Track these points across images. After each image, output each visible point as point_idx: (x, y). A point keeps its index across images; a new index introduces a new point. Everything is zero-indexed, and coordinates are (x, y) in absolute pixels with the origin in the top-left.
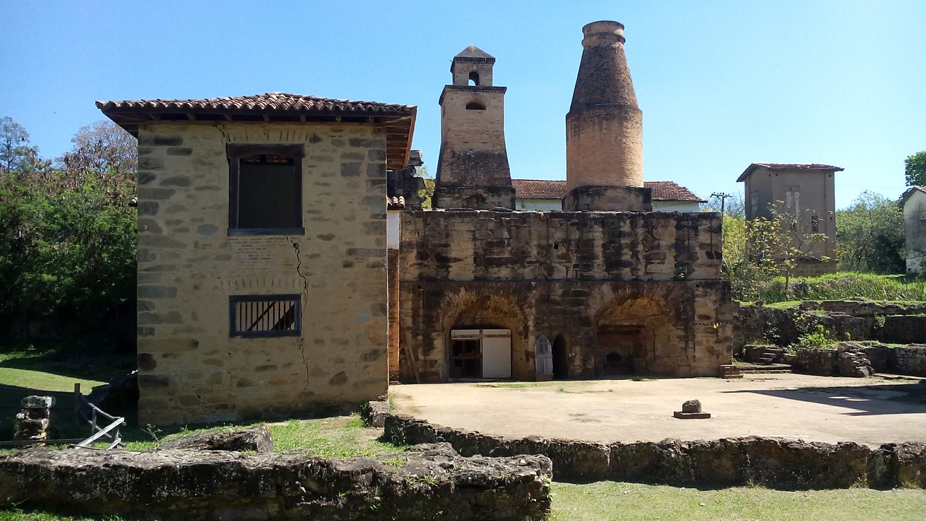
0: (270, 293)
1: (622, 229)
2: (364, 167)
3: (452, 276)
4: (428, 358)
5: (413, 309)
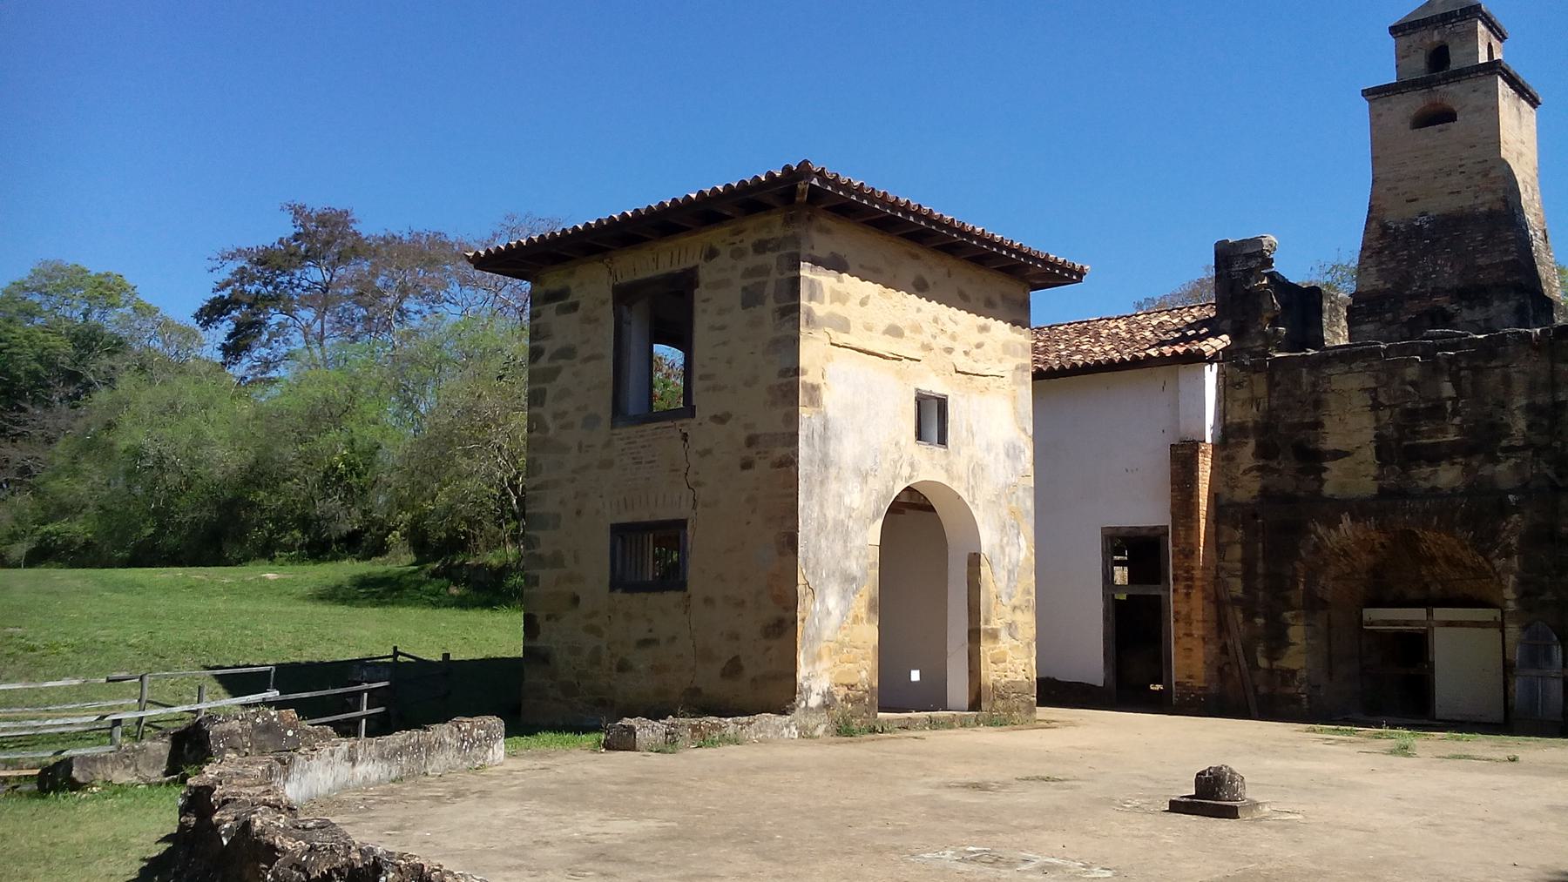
0: (653, 519)
2: (770, 289)
3: (1328, 490)
4: (1275, 664)
5: (1243, 561)
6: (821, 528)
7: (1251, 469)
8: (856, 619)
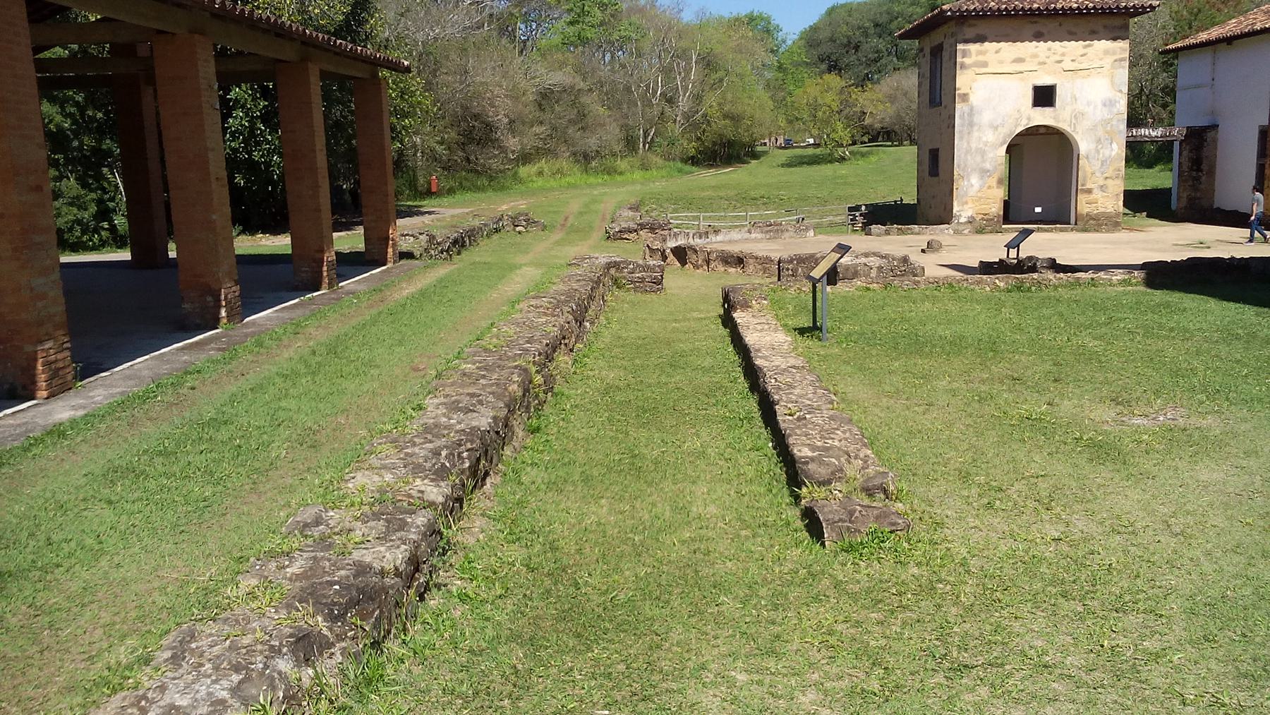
6: (968, 152)
8: (989, 187)
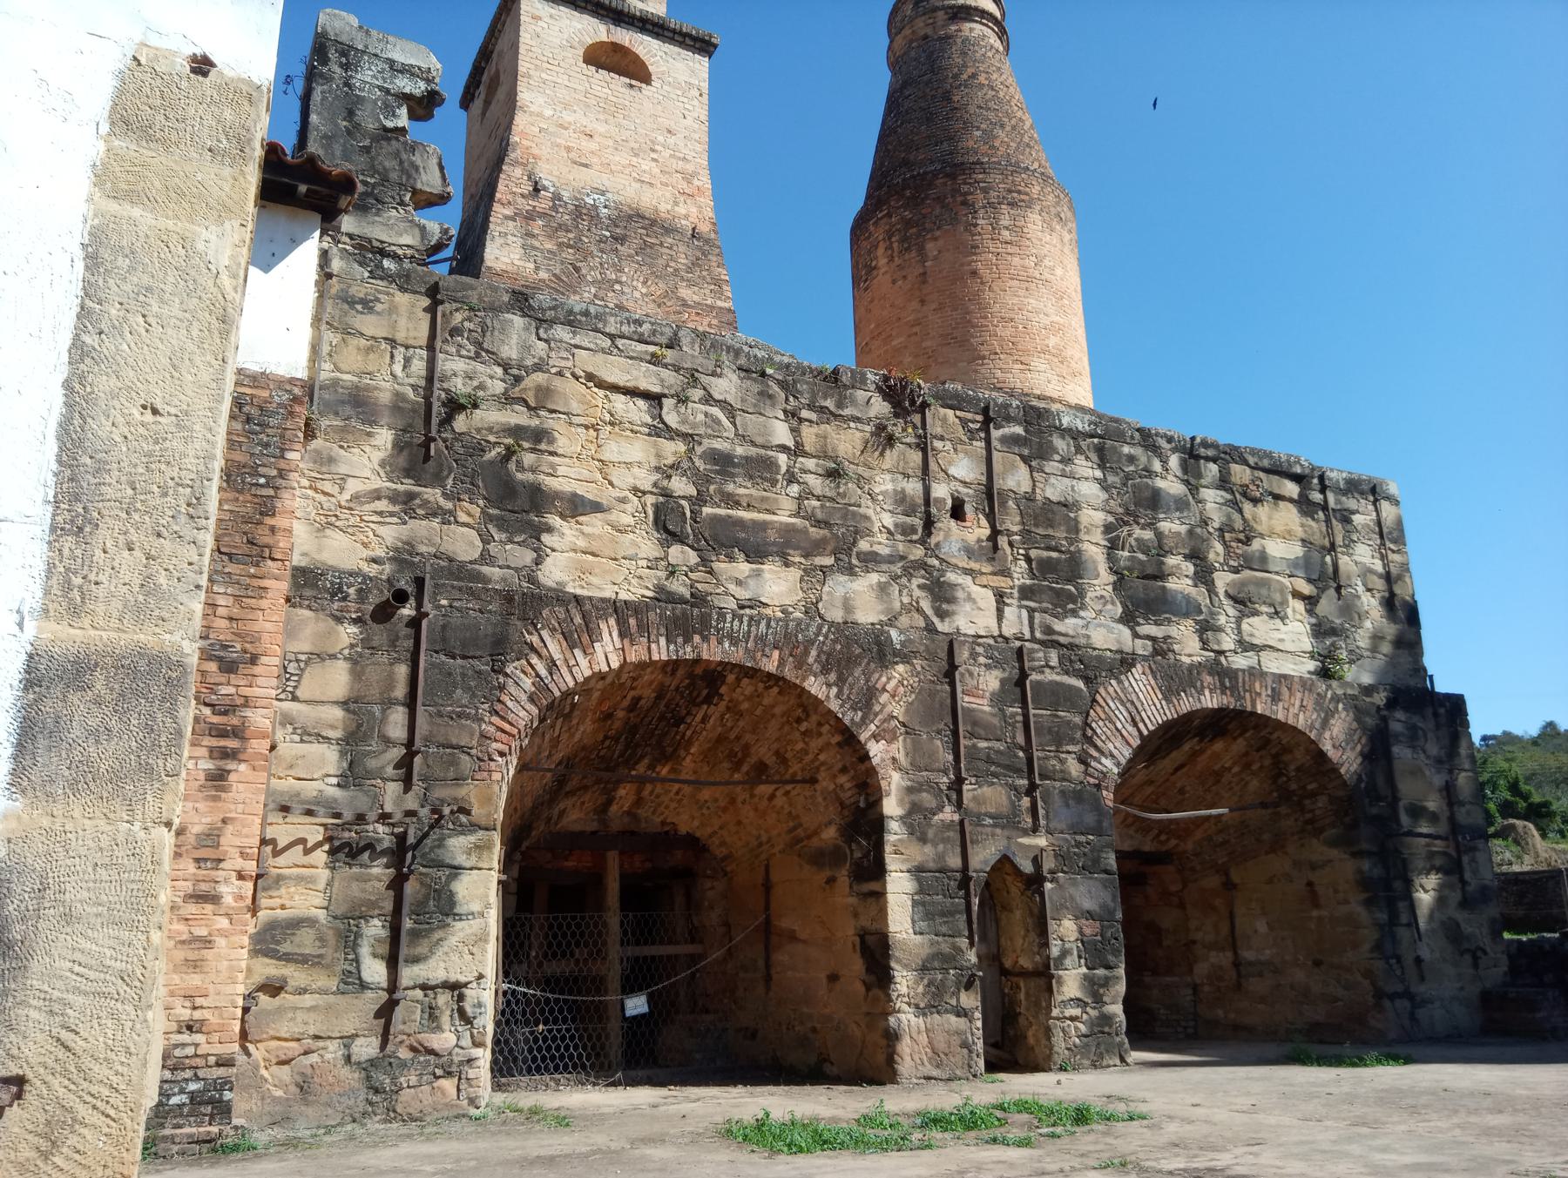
1: (1160, 483)
7: (376, 495)
